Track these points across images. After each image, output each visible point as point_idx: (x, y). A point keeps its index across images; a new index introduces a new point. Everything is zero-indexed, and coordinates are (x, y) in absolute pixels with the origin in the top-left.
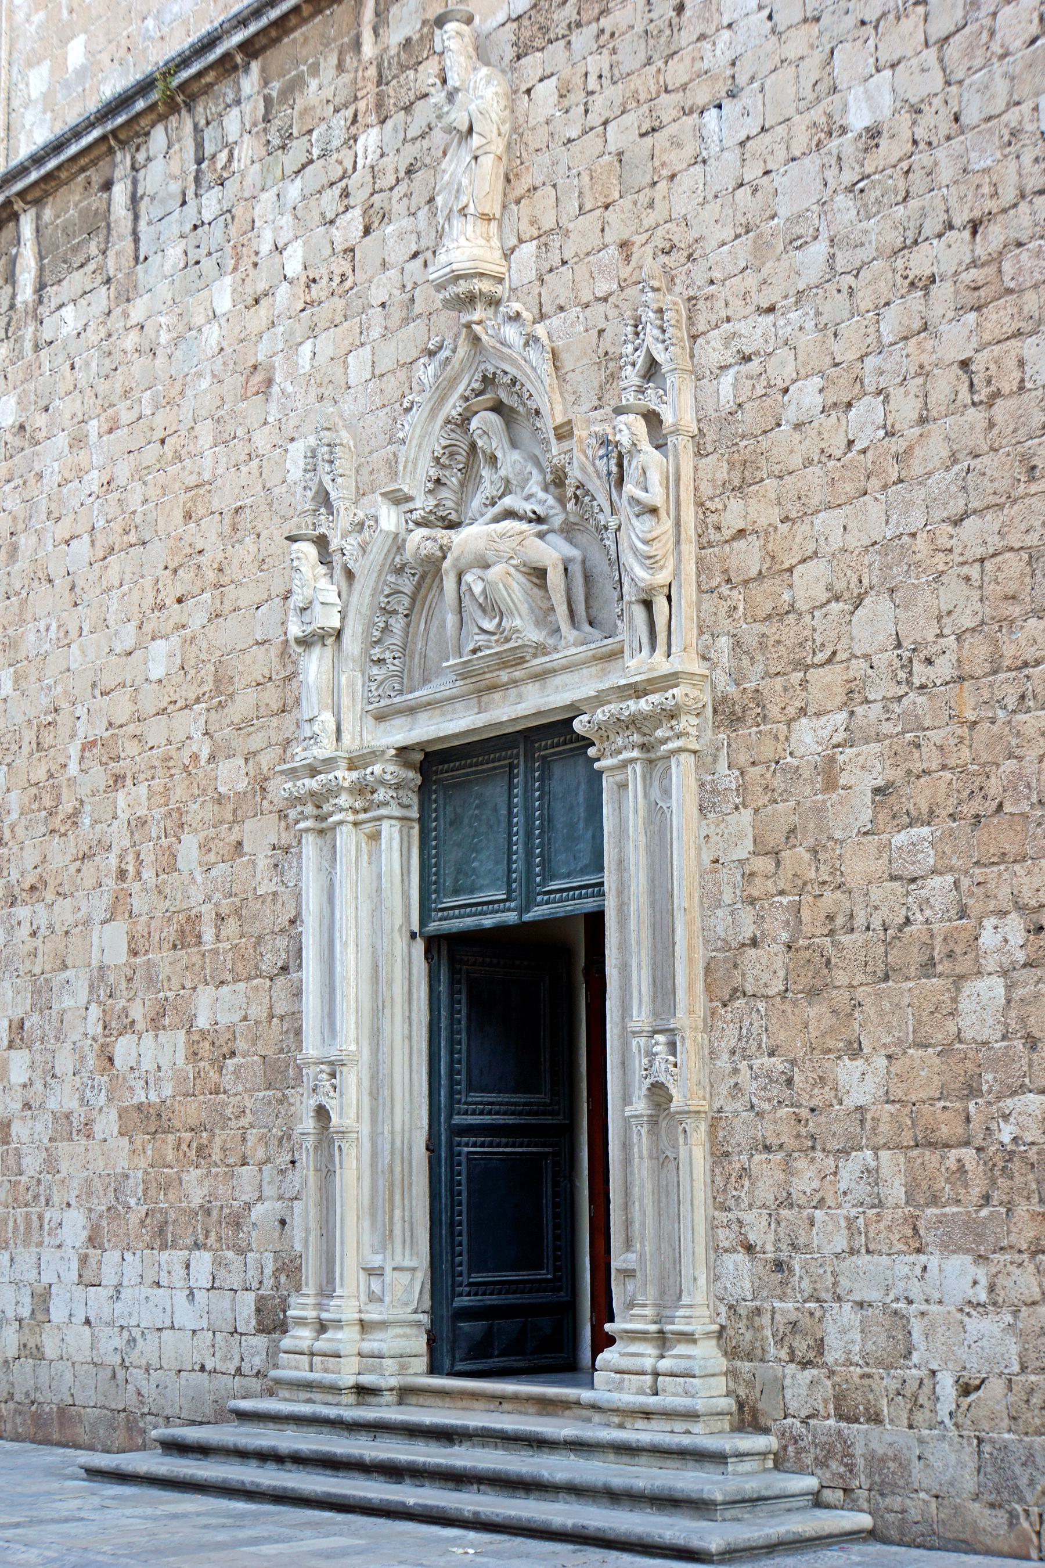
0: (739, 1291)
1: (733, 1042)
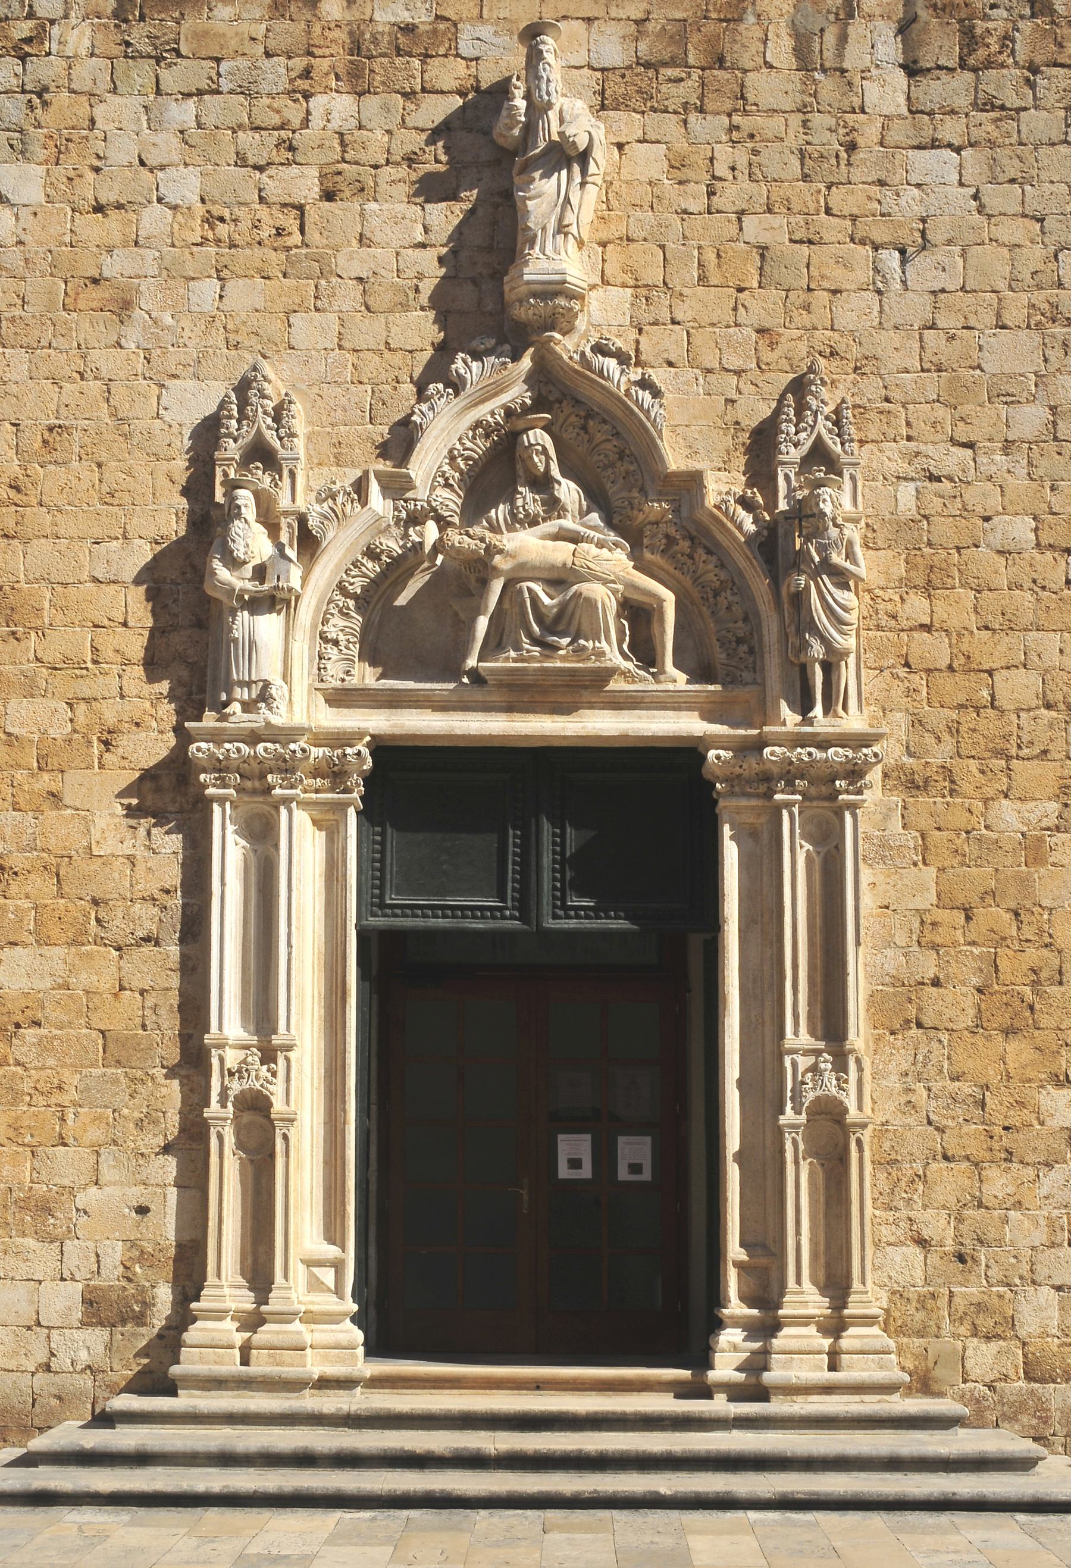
0: (909, 1279)
1: (905, 1066)
